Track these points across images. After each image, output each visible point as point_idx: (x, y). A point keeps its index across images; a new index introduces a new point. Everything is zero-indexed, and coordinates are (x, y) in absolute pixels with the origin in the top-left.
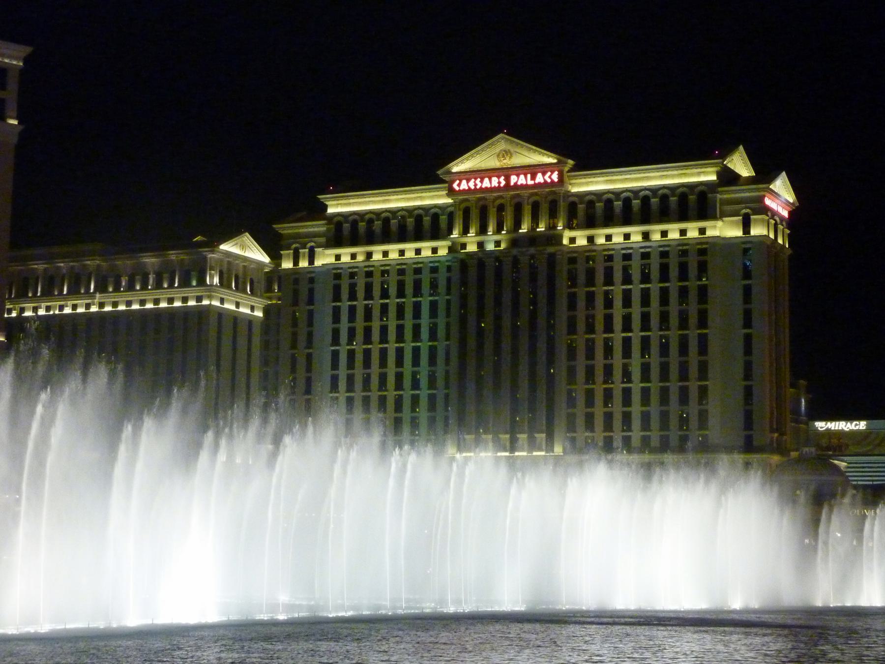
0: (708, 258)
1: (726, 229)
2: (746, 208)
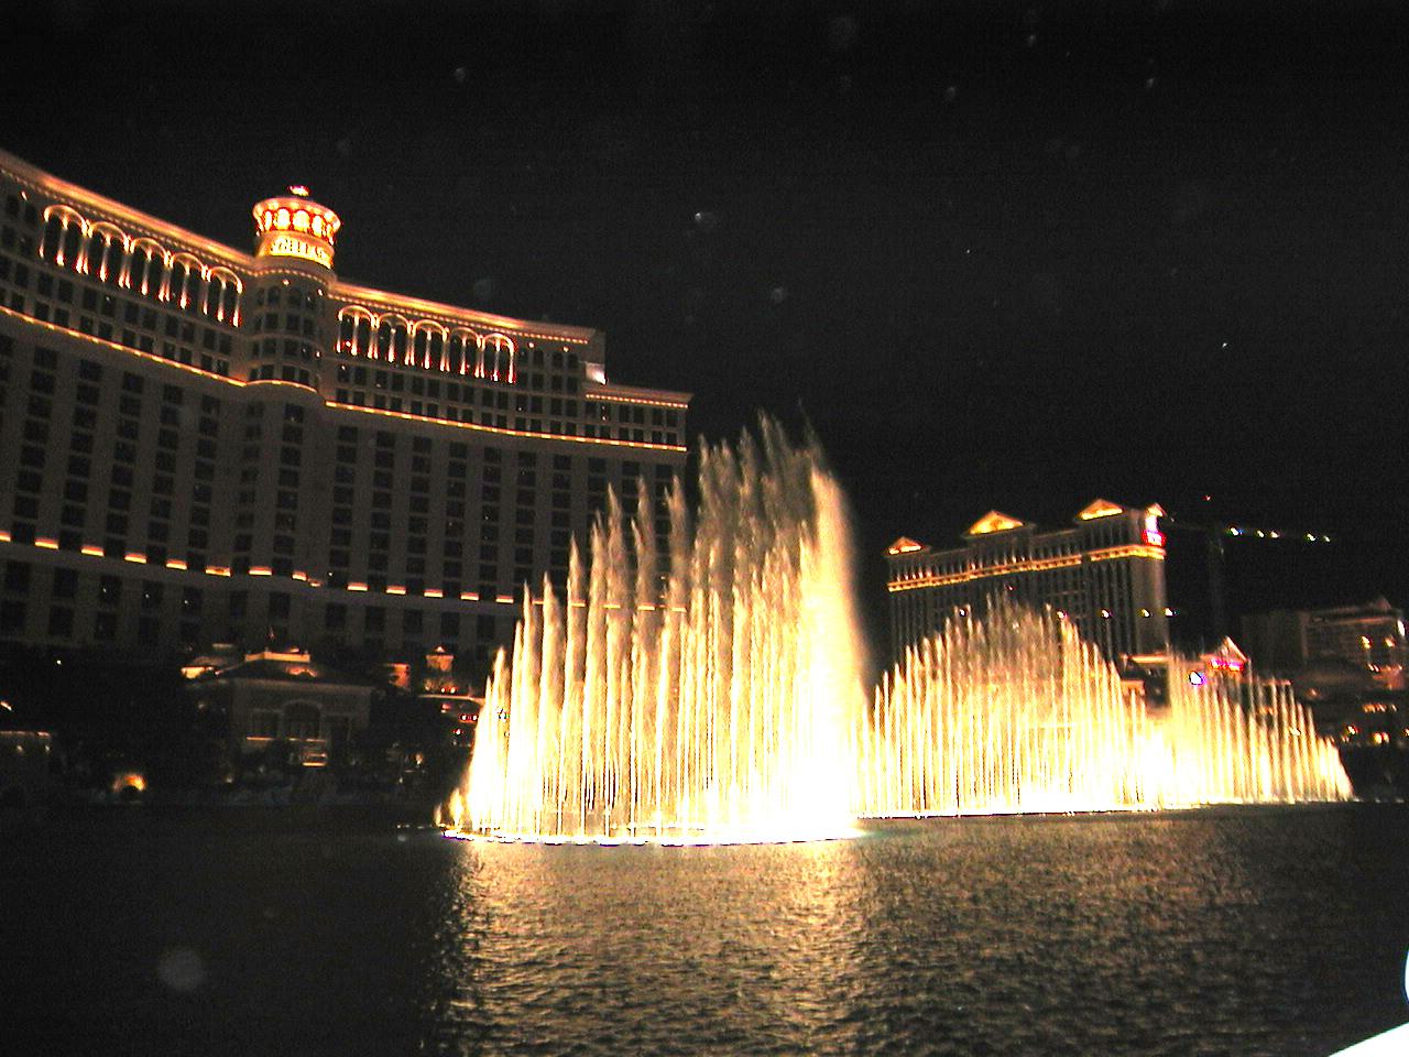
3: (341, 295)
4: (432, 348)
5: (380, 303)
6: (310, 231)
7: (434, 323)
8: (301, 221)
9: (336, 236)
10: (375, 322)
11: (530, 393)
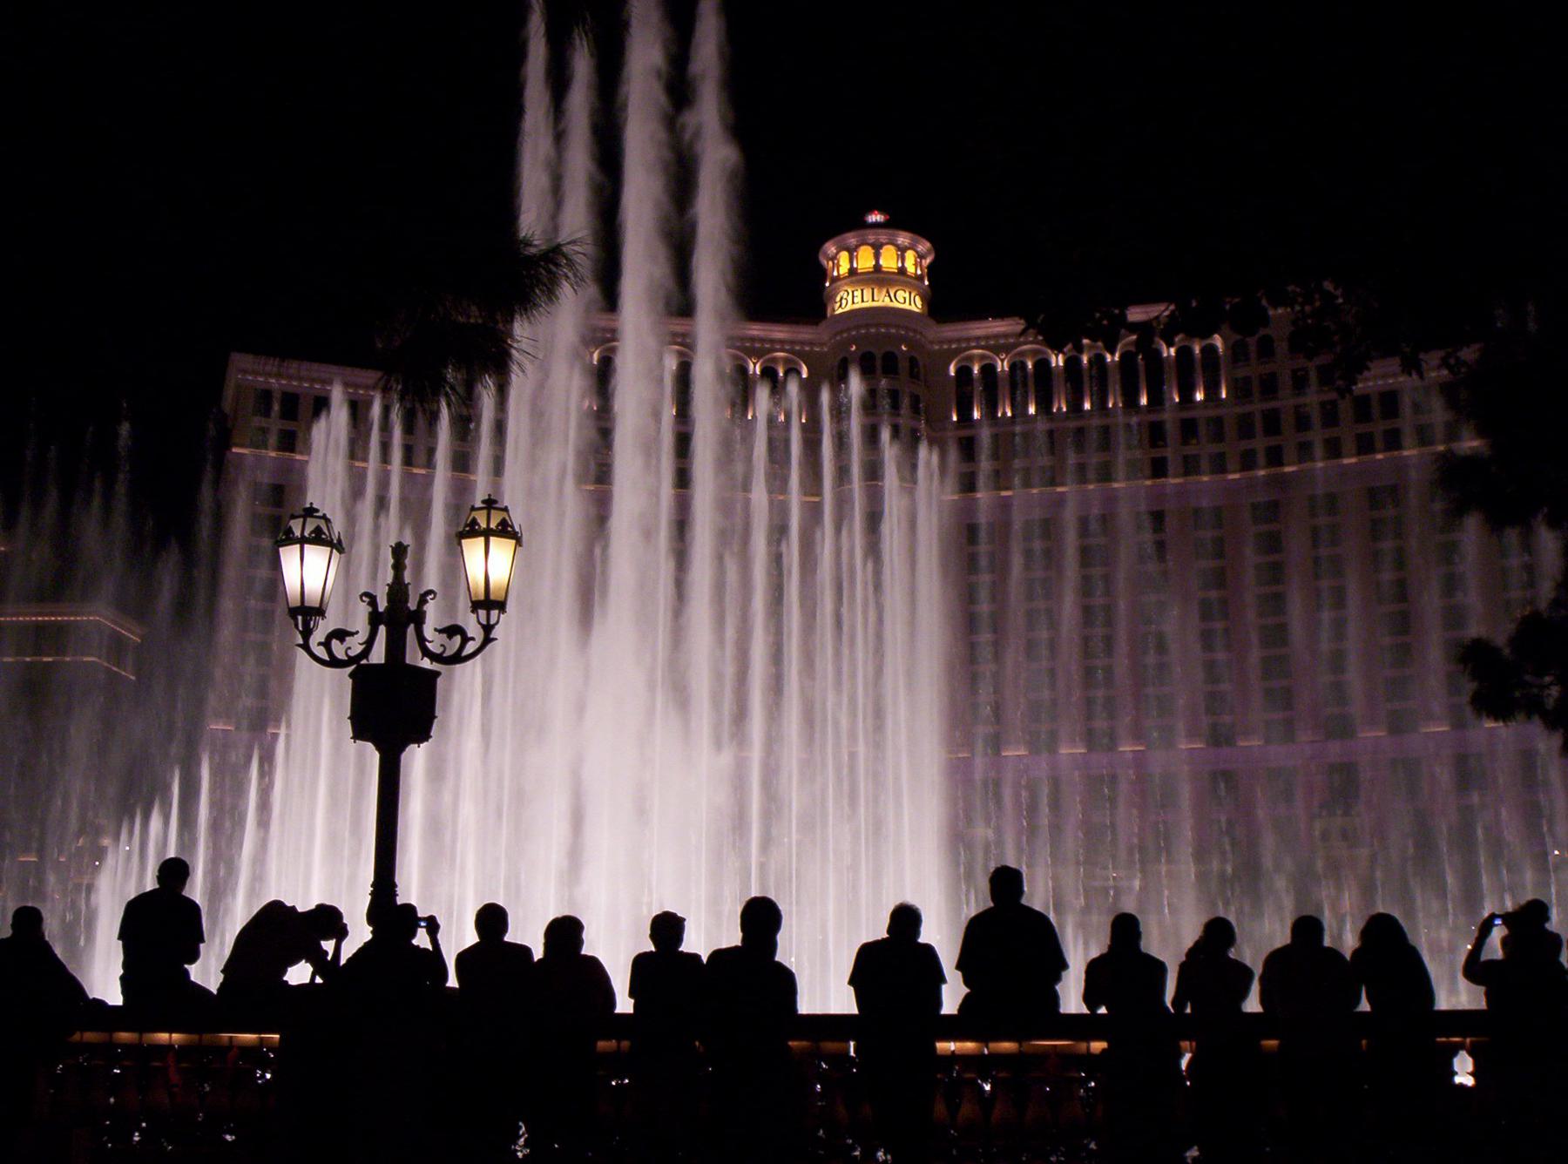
3: (950, 341)
4: (1037, 384)
5: (1006, 336)
6: (877, 268)
8: (865, 260)
10: (1002, 366)
11: (1257, 407)
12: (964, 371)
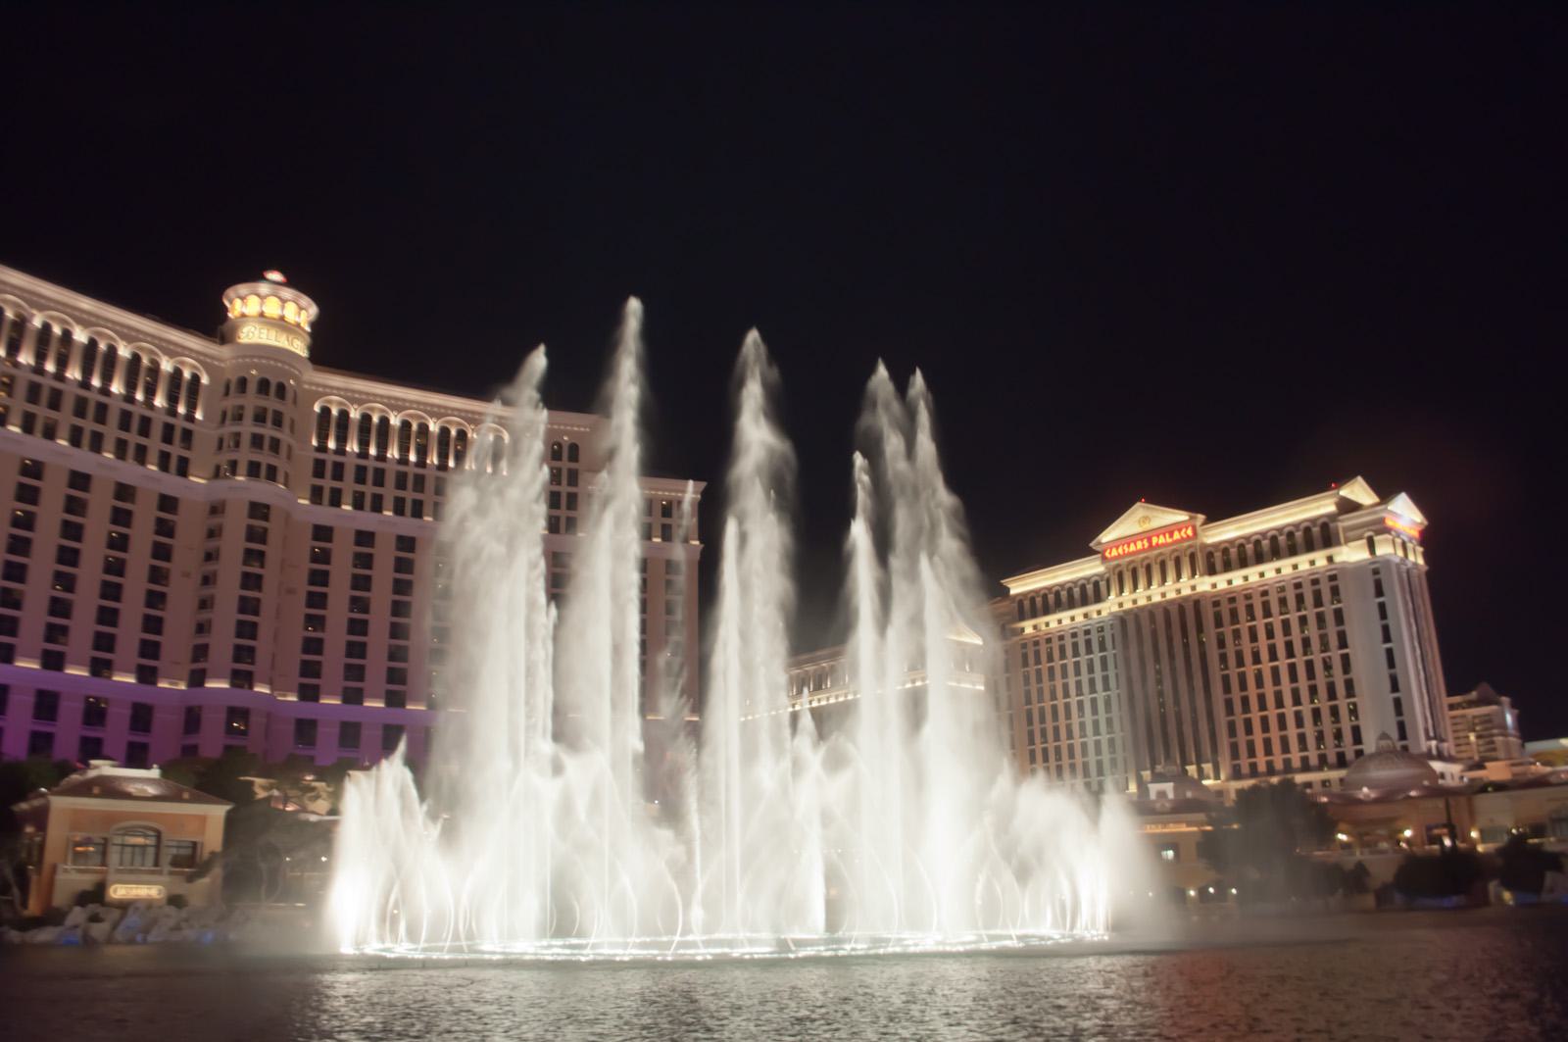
0: (1340, 583)
1: (1351, 554)
2: (1369, 530)
3: (318, 385)
6: (282, 318)
7: (420, 413)
8: (272, 308)
9: (314, 325)
12: (326, 411)
